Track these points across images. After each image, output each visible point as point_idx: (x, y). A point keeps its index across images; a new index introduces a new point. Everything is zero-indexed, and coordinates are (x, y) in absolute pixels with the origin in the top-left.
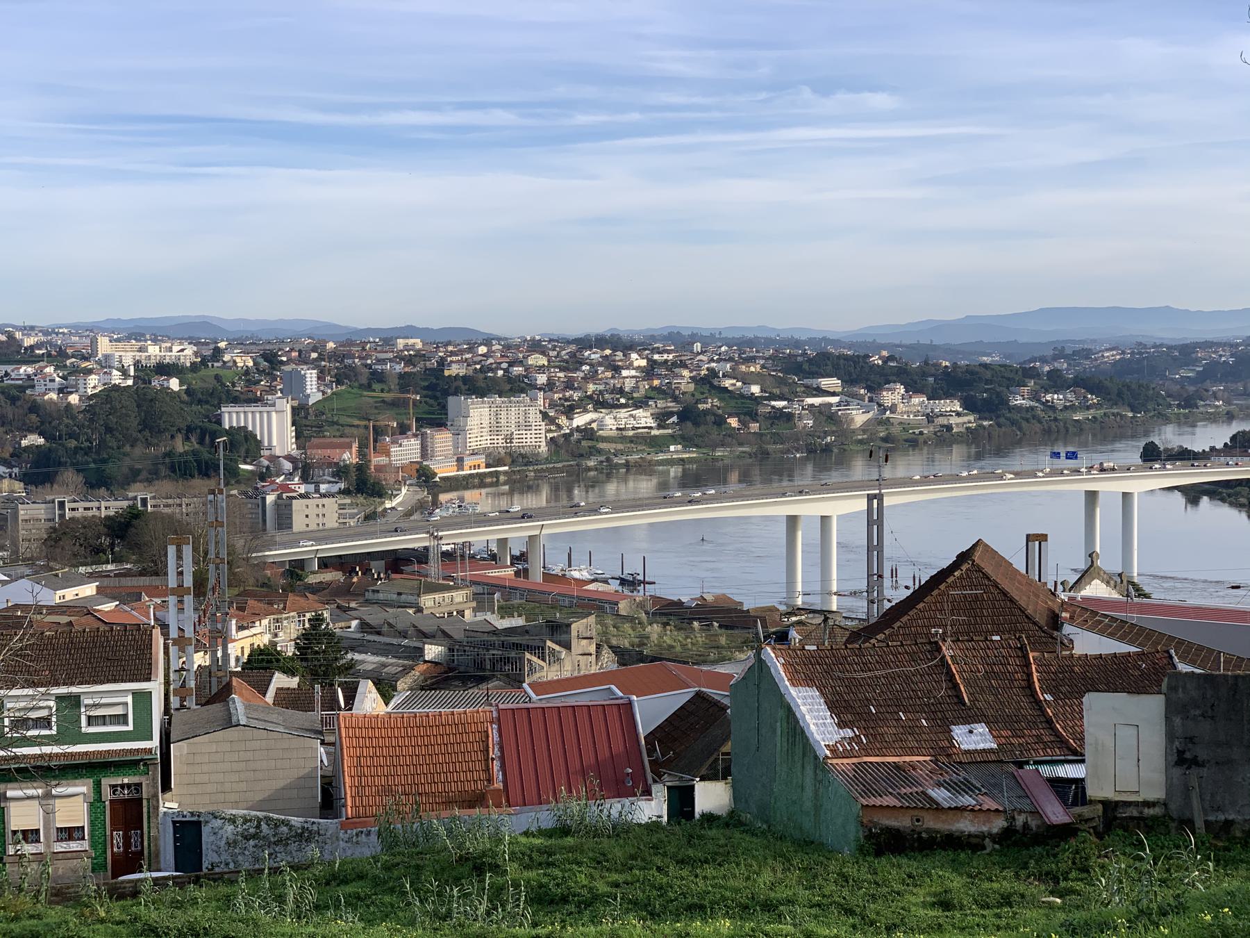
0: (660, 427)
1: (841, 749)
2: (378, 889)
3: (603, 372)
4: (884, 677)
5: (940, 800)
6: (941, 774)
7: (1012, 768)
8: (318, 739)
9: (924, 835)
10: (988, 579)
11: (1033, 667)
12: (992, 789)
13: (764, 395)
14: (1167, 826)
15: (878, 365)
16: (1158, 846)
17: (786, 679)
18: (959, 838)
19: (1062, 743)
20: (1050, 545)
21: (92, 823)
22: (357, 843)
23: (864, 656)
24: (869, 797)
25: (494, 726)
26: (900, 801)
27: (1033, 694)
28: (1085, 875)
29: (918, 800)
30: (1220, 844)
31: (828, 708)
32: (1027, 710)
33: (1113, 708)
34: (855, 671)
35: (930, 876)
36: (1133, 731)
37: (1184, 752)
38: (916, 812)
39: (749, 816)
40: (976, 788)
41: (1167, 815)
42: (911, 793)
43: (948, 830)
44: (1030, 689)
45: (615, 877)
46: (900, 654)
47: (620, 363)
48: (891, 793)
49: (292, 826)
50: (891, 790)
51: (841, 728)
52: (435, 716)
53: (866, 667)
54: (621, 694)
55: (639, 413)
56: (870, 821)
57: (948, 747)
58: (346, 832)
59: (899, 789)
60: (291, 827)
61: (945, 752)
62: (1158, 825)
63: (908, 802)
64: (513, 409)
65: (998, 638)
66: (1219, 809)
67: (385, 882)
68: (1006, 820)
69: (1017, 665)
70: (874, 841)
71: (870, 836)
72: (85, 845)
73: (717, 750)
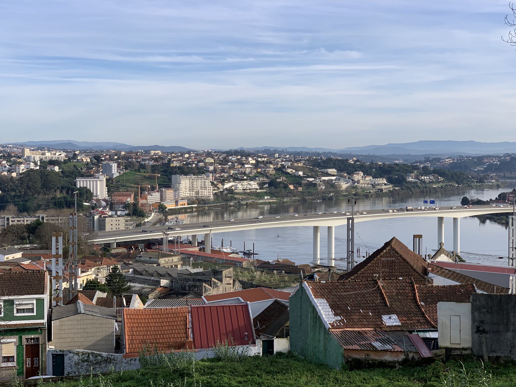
0: (261, 189)
1: (336, 325)
2: (139, 383)
3: (237, 166)
4: (354, 295)
5: (377, 347)
6: (378, 336)
7: (408, 333)
8: (114, 319)
9: (370, 362)
10: (398, 254)
11: (416, 291)
12: (399, 342)
14: (472, 358)
16: (468, 367)
17: (313, 295)
18: (385, 363)
19: (428, 322)
20: (424, 240)
21: (18, 355)
22: (130, 364)
23: (345, 286)
24: (347, 345)
25: (189, 314)
26: (360, 347)
27: (416, 302)
28: (438, 379)
29: (368, 347)
30: (495, 366)
31: (330, 307)
32: (414, 309)
33: (450, 308)
34: (342, 292)
35: (373, 379)
36: (458, 318)
37: (479, 327)
38: (366, 352)
39: (296, 353)
40: (392, 342)
41: (473, 354)
42: (365, 344)
43: (381, 360)
44: (415, 300)
45: (240, 379)
46: (361, 285)
47: (244, 162)
48: (356, 344)
49: (103, 356)
50: (356, 342)
51: (336, 316)
52: (164, 310)
53: (346, 290)
54: (243, 301)
55: (252, 183)
56: (348, 356)
57: (380, 324)
58: (126, 359)
59: (360, 342)
60: (102, 357)
61: (379, 326)
62: (468, 358)
63: (364, 348)
64: (199, 181)
65: (401, 278)
66: (494, 351)
67: (142, 381)
68: (405, 355)
69: (409, 290)
70: (349, 364)
71: (347, 362)
72: (14, 364)
73: (283, 325)
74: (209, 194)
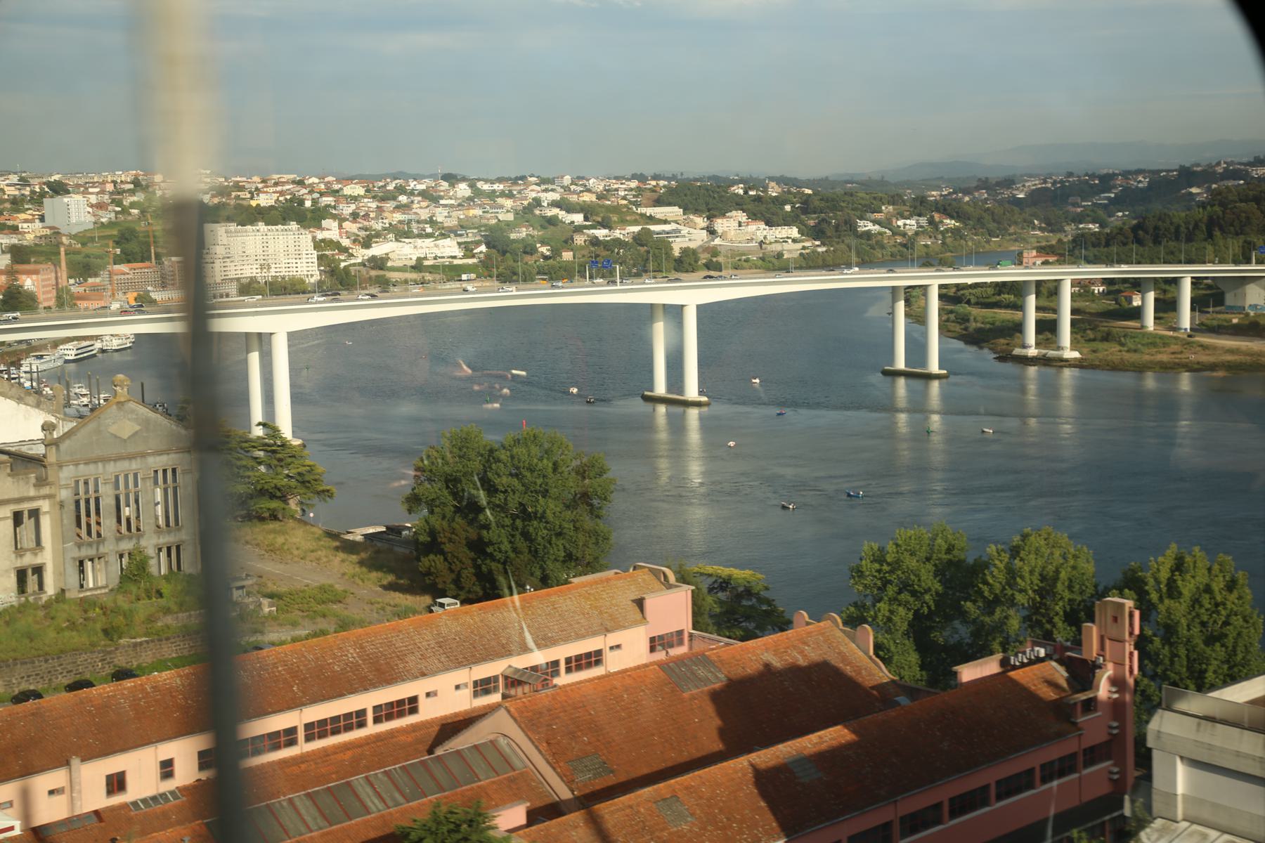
0: (465, 257)
3: (419, 202)
13: (587, 223)
15: (737, 195)
47: (442, 194)
55: (447, 242)
64: (281, 237)
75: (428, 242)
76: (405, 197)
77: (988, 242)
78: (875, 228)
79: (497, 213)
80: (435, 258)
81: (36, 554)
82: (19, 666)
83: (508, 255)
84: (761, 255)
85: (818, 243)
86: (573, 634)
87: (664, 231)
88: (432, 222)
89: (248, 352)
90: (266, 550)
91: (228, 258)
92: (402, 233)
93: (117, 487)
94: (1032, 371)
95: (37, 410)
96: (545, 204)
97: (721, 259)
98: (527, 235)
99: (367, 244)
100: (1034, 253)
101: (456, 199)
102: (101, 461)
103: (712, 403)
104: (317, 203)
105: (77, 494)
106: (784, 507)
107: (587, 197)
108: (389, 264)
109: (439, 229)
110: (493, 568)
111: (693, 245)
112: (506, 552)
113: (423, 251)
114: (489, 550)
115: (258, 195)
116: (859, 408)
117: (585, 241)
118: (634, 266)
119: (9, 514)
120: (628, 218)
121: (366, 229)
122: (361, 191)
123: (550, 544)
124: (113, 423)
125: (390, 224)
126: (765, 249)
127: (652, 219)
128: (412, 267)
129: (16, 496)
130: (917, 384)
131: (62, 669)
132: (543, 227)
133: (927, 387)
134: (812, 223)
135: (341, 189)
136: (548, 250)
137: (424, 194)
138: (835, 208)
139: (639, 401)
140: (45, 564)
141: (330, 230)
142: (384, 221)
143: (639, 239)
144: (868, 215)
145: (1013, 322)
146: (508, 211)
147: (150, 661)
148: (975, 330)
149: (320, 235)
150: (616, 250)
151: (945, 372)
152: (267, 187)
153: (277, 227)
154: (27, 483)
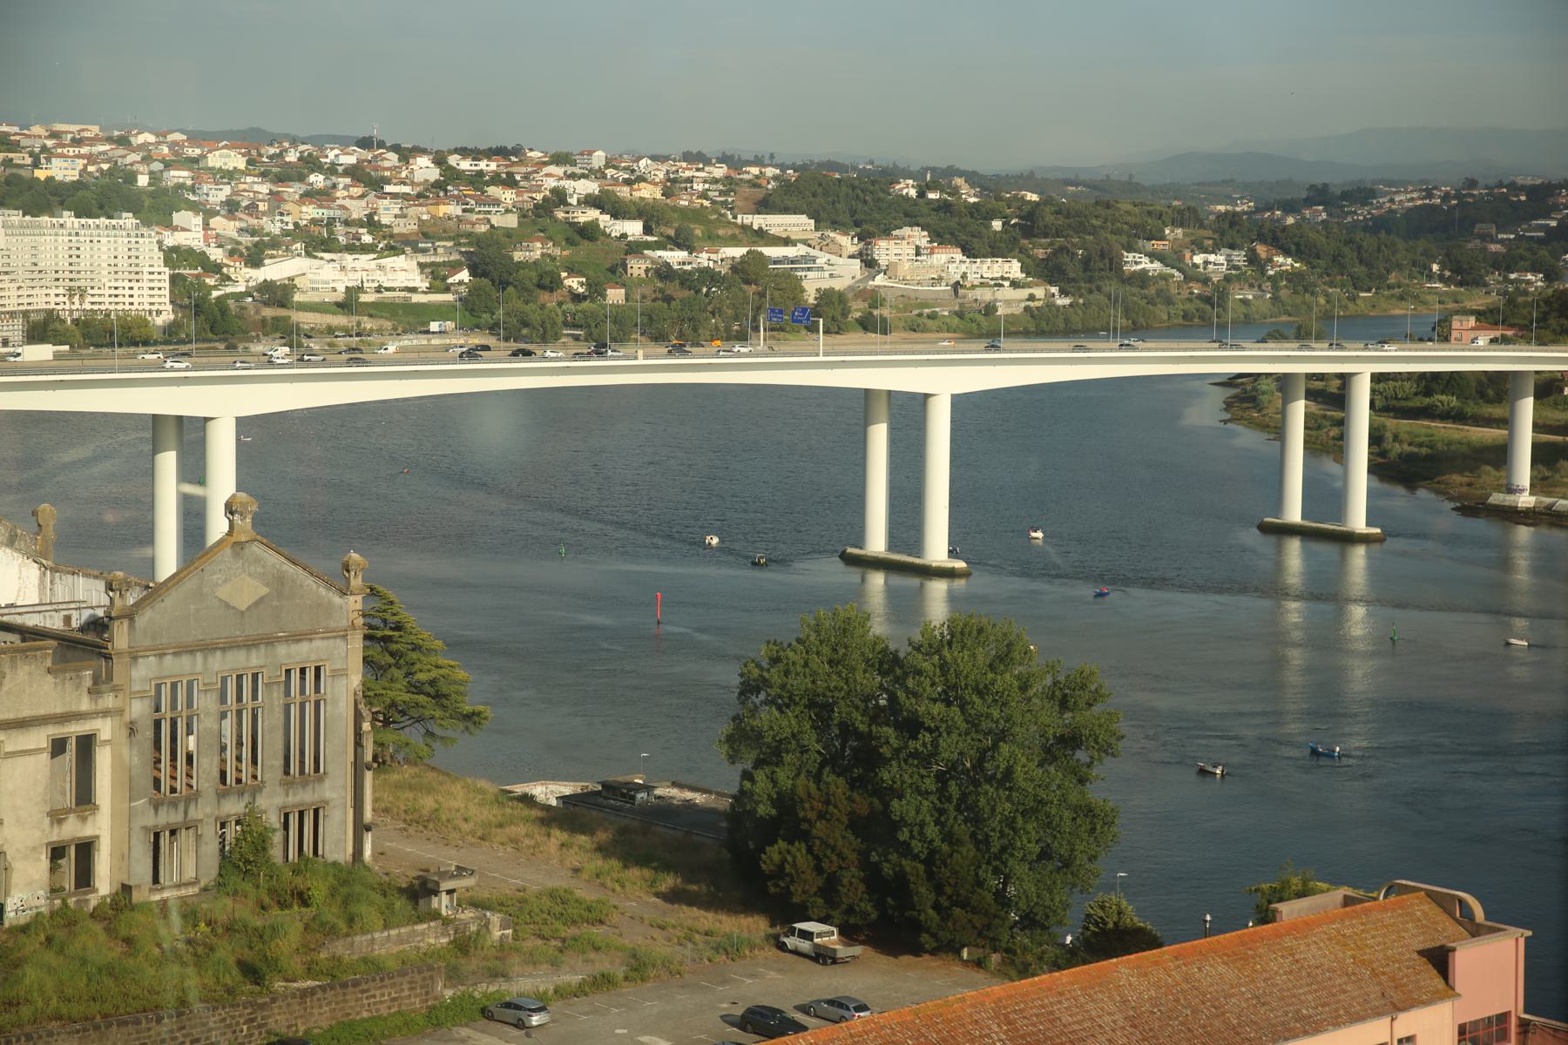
0: (431, 289)
3: (346, 187)
13: (650, 238)
15: (907, 198)
47: (387, 174)
55: (399, 261)
64: (104, 240)
74: (152, 300)
75: (365, 260)
76: (321, 178)
77: (1353, 299)
78: (1155, 267)
79: (489, 212)
80: (379, 290)
81: (84, 819)
82: (115, 1028)
83: (510, 289)
84: (957, 308)
85: (1054, 290)
86: (1342, 1012)
87: (786, 257)
88: (371, 223)
89: (156, 450)
90: (405, 821)
91: (6, 273)
92: (318, 242)
93: (223, 700)
94: (1524, 533)
95: (8, 551)
96: (574, 201)
97: (886, 312)
98: (543, 255)
99: (255, 261)
100: (1472, 321)
101: (413, 184)
102: (200, 650)
103: (975, 573)
104: (161, 180)
105: (158, 709)
106: (1203, 772)
107: (647, 192)
108: (297, 298)
109: (384, 238)
110: (908, 869)
111: (838, 285)
112: (932, 841)
113: (358, 276)
114: (903, 835)
115: (48, 160)
116: (1243, 590)
117: (647, 271)
118: (736, 318)
119: (44, 744)
120: (721, 232)
121: (253, 233)
122: (241, 163)
123: (1013, 829)
124: (225, 581)
125: (296, 225)
126: (964, 297)
127: (762, 236)
128: (338, 304)
129: (59, 710)
130: (1327, 550)
131: (184, 1036)
132: (570, 242)
133: (1343, 559)
134: (1040, 253)
135: (203, 156)
136: (582, 284)
137: (355, 173)
138: (1081, 229)
139: (837, 565)
140: (97, 837)
141: (189, 232)
142: (286, 219)
143: (740, 269)
144: (1141, 243)
145: (1469, 444)
146: (507, 211)
147: (325, 1024)
148: (1400, 456)
149: (171, 239)
150: (705, 290)
151: (1378, 531)
152: (64, 146)
153: (97, 221)
154: (78, 686)
